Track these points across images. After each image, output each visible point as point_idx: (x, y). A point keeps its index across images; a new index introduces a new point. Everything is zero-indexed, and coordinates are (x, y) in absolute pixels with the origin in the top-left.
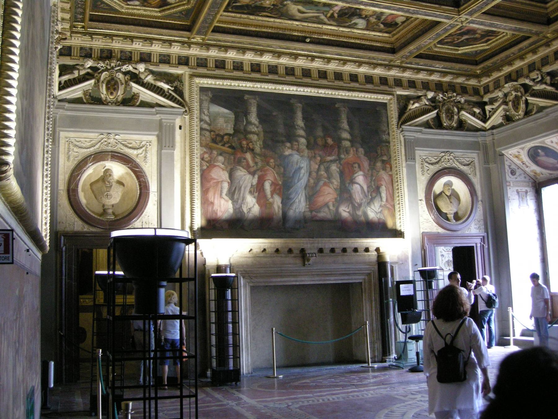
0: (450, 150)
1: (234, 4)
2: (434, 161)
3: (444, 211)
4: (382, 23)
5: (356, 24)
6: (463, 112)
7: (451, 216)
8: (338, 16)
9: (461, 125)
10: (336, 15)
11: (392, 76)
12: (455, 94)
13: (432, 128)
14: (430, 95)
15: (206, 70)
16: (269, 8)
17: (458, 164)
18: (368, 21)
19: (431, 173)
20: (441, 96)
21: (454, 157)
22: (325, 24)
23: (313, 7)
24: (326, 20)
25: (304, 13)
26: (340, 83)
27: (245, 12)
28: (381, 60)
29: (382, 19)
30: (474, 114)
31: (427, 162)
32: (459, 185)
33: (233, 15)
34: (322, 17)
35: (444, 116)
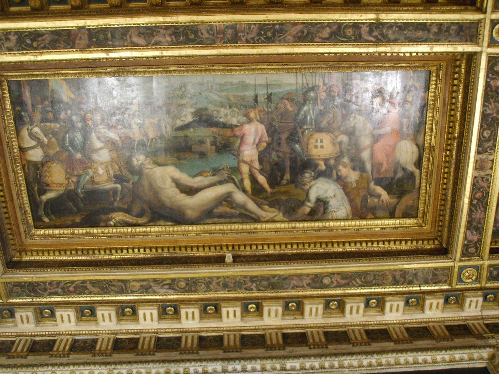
1: (45, 198)
4: (379, 182)
5: (322, 203)
8: (271, 185)
10: (262, 179)
11: (475, 318)
15: (5, 358)
16: (115, 191)
18: (340, 180)
22: (257, 220)
23: (200, 163)
24: (252, 206)
25: (191, 191)
26: (344, 346)
27: (78, 220)
28: (426, 283)
29: (368, 167)
33: (56, 232)
34: (240, 197)
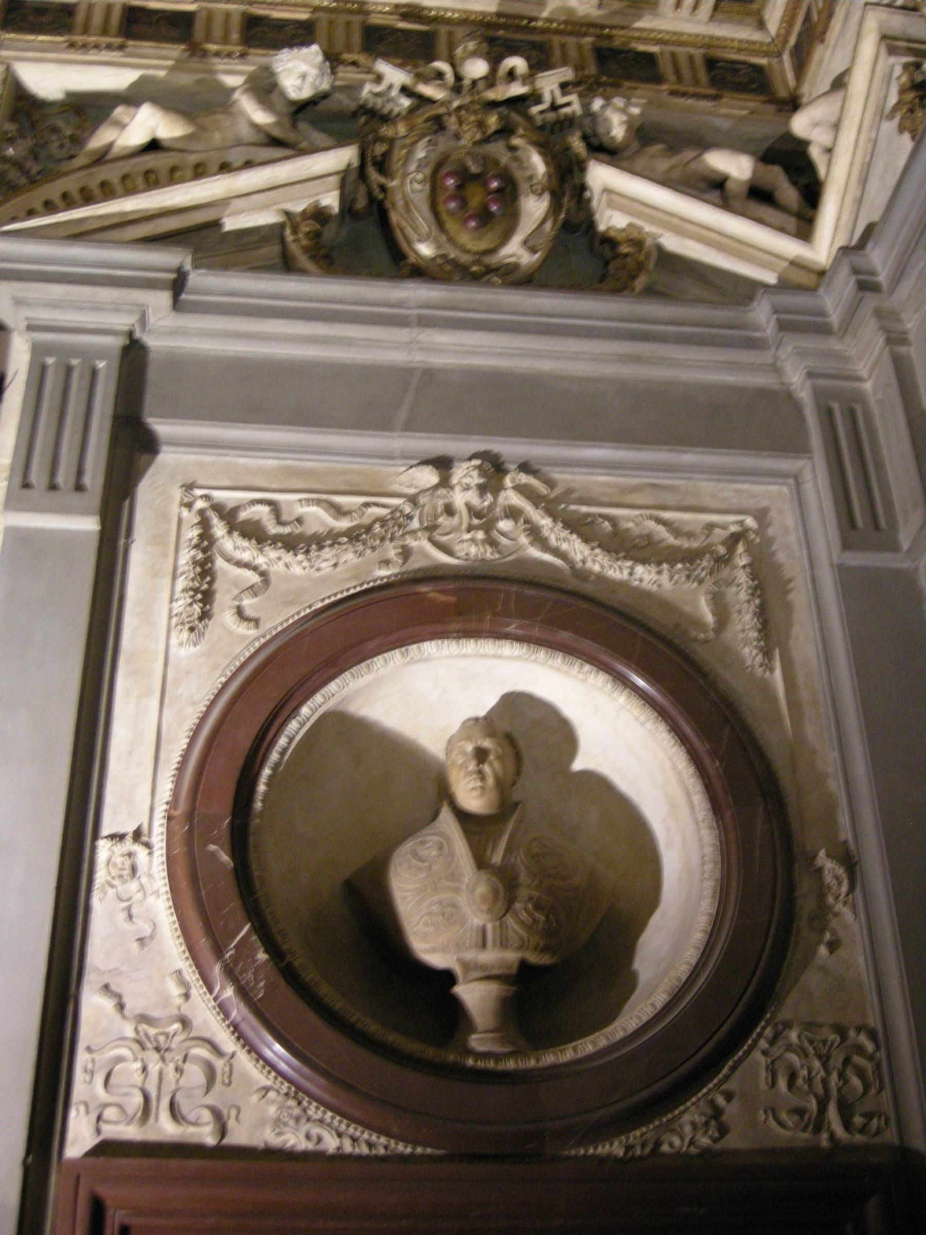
0: (511, 449)
2: (318, 518)
3: (430, 946)
6: (601, 176)
7: (474, 995)
9: (589, 257)
12: (517, 63)
13: (303, 272)
14: (299, 72)
17: (577, 549)
19: (278, 618)
20: (394, 75)
21: (550, 507)
30: (715, 188)
31: (253, 532)
32: (620, 738)
35: (410, 187)
